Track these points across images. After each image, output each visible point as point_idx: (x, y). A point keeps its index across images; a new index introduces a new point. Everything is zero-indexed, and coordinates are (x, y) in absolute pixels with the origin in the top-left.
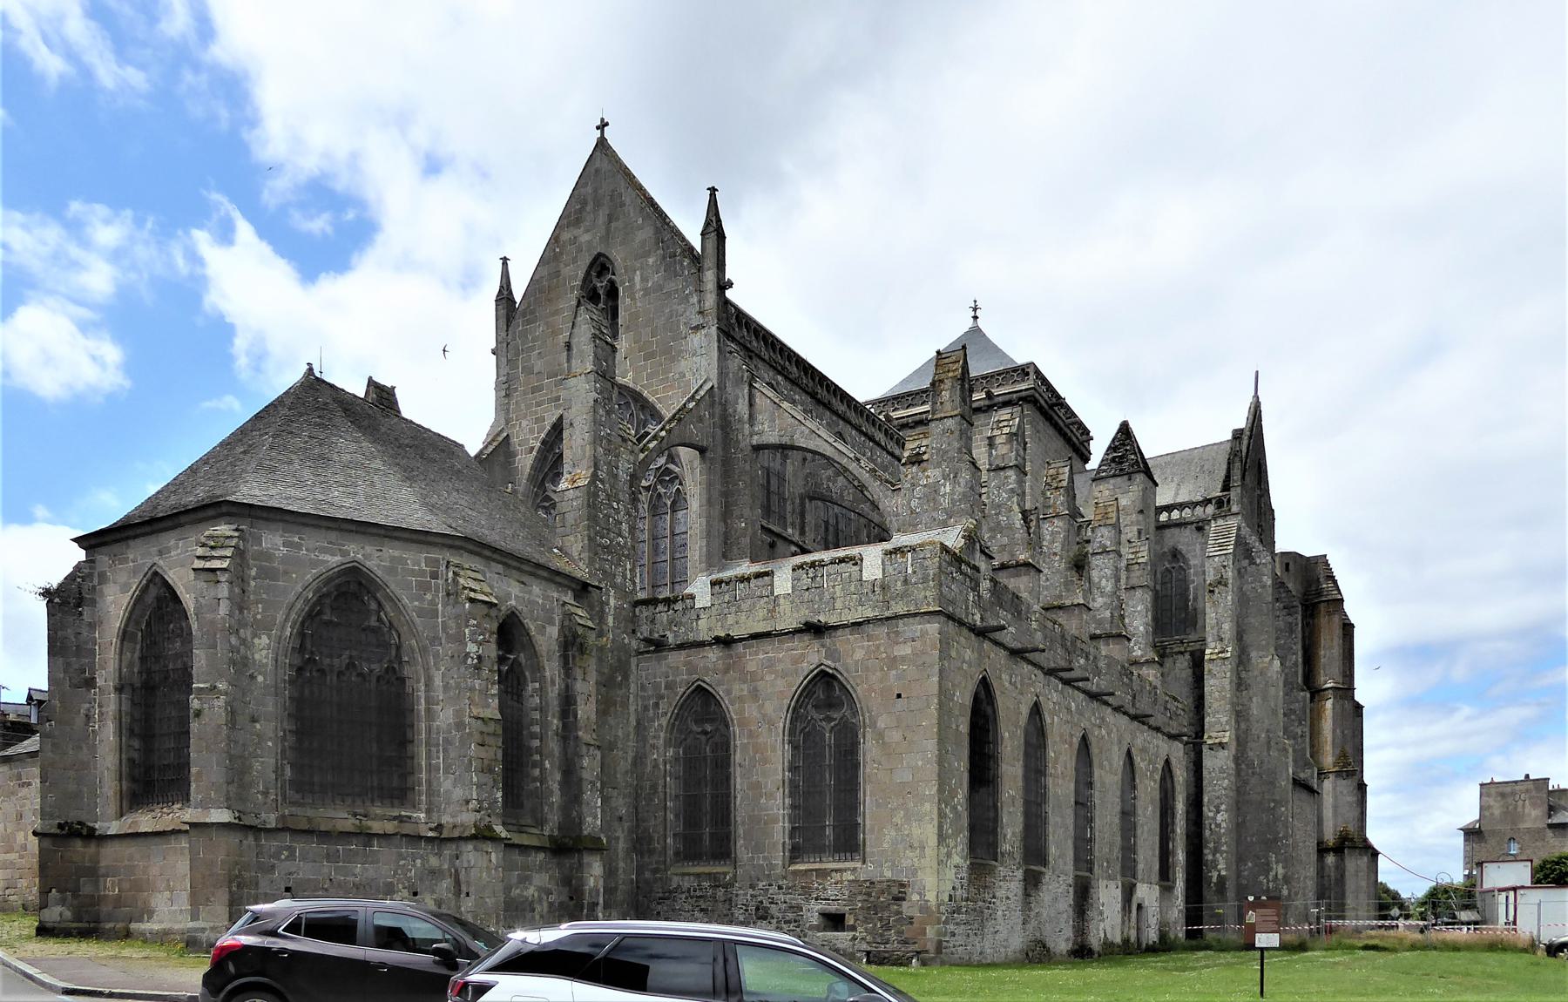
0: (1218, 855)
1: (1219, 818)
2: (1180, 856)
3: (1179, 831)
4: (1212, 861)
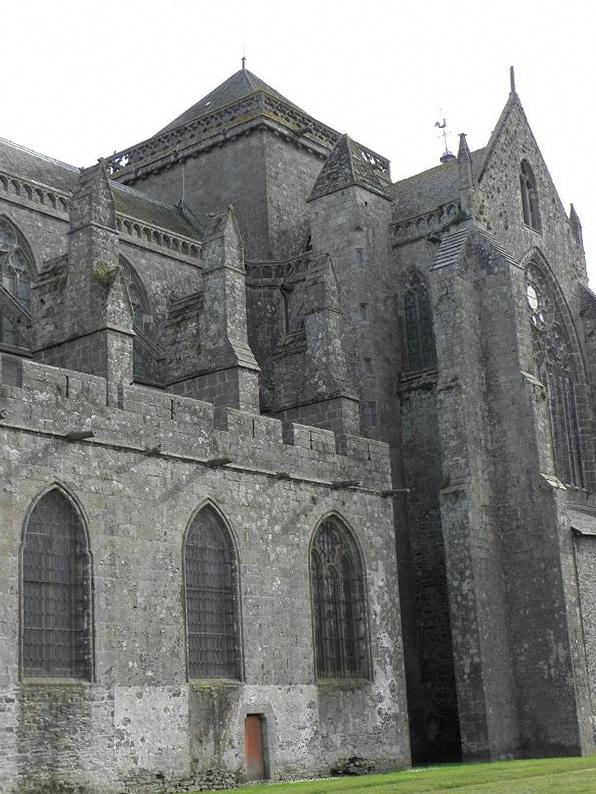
0: (468, 636)
1: (465, 587)
2: (385, 640)
3: (377, 608)
4: (463, 645)
